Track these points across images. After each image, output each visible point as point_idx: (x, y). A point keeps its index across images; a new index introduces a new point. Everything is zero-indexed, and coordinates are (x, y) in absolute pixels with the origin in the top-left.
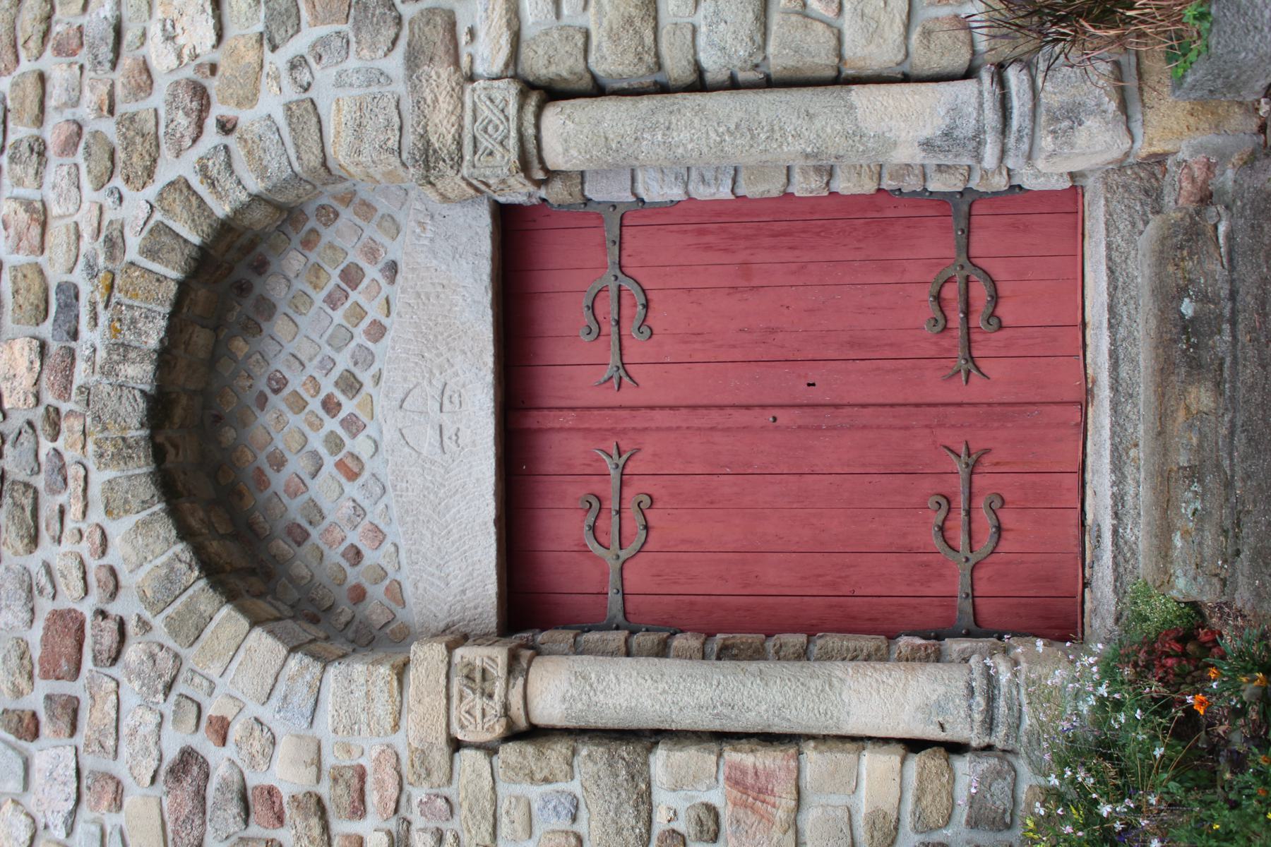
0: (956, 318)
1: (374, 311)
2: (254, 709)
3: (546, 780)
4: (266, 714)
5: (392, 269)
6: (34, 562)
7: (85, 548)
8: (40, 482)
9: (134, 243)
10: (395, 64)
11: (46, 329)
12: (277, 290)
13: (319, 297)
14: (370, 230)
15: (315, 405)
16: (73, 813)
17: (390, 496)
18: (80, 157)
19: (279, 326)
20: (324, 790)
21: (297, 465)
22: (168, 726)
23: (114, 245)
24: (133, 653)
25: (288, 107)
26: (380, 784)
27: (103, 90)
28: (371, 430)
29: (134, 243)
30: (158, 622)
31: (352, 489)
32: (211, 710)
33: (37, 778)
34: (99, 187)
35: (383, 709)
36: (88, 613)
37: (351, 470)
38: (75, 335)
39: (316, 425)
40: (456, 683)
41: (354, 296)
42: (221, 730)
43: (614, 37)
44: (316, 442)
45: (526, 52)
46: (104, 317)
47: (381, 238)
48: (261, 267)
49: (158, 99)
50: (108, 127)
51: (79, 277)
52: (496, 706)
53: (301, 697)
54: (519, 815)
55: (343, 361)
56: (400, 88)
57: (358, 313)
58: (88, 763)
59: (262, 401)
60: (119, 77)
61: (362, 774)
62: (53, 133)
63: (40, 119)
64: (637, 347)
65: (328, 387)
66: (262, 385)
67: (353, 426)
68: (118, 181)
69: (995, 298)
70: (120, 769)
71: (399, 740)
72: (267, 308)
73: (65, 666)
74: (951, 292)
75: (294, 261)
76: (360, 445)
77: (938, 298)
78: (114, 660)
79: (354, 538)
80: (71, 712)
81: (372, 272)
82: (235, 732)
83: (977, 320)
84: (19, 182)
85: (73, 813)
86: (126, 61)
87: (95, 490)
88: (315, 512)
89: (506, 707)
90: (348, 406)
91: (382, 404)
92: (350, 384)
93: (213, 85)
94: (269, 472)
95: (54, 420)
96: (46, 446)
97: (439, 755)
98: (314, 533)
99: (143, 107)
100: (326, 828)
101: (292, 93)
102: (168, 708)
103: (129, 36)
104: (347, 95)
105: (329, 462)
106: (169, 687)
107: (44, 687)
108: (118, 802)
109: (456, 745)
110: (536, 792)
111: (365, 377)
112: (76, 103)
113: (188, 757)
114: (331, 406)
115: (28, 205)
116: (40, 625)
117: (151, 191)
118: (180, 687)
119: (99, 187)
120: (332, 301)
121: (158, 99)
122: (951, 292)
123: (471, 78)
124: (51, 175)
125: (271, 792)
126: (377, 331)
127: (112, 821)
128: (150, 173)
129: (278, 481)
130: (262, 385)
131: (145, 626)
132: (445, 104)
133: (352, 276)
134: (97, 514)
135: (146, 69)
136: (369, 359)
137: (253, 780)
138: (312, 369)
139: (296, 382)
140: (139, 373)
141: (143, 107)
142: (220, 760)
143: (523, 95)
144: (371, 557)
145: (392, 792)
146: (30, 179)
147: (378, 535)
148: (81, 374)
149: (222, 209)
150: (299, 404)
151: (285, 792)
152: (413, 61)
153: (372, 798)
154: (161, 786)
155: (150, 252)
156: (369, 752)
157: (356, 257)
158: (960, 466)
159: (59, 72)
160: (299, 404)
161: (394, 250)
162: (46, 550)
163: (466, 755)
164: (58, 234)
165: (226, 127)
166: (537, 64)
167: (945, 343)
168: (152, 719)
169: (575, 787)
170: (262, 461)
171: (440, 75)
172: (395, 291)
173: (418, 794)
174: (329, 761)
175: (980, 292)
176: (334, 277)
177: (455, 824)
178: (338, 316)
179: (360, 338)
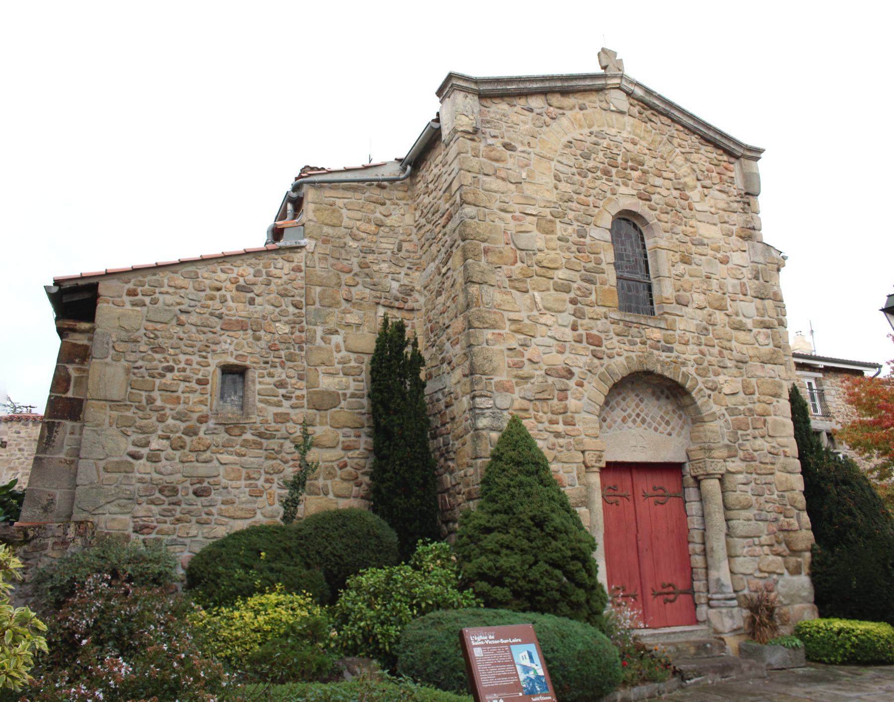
0: (666, 590)
1: (660, 429)
2: (586, 395)
3: (578, 478)
4: (585, 398)
5: (670, 434)
6: (612, 334)
7: (617, 349)
8: (630, 338)
9: (684, 369)
10: (726, 442)
11: (663, 343)
12: (663, 401)
13: (662, 413)
14: (677, 429)
15: (637, 411)
16: (555, 338)
17: (619, 431)
18: (699, 355)
19: (656, 402)
20: (569, 414)
21: (623, 404)
22: (580, 370)
23: (684, 364)
24: (596, 361)
25: (714, 413)
26: (574, 430)
27: (714, 363)
28: (634, 427)
29: (684, 369)
30: (603, 369)
31: (619, 420)
32: (585, 382)
33: (563, 329)
34: (695, 360)
35: (590, 432)
36: (603, 348)
37: (624, 420)
38: (663, 351)
39: (633, 410)
40: (598, 453)
41: (663, 423)
42: (580, 385)
43: (737, 498)
44: (629, 411)
45: (731, 475)
46: (668, 360)
47: (676, 431)
48: (667, 398)
49: (713, 378)
50: (706, 364)
51: (674, 354)
52: (594, 464)
53: (591, 409)
54: (570, 469)
55: (648, 419)
56: (722, 443)
57: (660, 425)
58: (568, 344)
59: (637, 396)
60: (716, 367)
61: (574, 425)
62: (703, 347)
63: (706, 345)
64: (652, 499)
65: (642, 415)
66: (641, 396)
67: (634, 421)
68: (696, 366)
69: (671, 601)
70: (567, 354)
71: (583, 436)
72: (658, 399)
73: (591, 341)
74: (671, 589)
75: (670, 408)
76: (630, 423)
77: (670, 585)
78: (594, 356)
79: (608, 420)
80: (580, 342)
81: (669, 429)
82: (580, 389)
83: (666, 596)
84: (693, 338)
85: (555, 338)
86: (720, 370)
87: (631, 354)
88: (613, 409)
89: (593, 467)
90: (639, 420)
91: (640, 430)
92: (643, 421)
93: (716, 392)
94: (621, 396)
95: (644, 343)
96: (638, 340)
97: (581, 448)
98: (608, 409)
99: (711, 374)
100: (560, 413)
101: (718, 413)
102: (583, 370)
103: (725, 370)
104: (718, 429)
105: (625, 414)
106: (590, 371)
107: (584, 333)
108: (559, 352)
109: (583, 452)
110: (575, 474)
111: (645, 426)
112: (710, 355)
113: (571, 374)
114: (638, 415)
115: (688, 341)
116: (597, 333)
117: (695, 375)
118: (589, 374)
119: (695, 360)
120: (662, 417)
121: (713, 378)
122: (671, 589)
123: (725, 461)
124: (695, 347)
125: (567, 398)
126: (656, 429)
127: (554, 349)
128: (699, 375)
129: (619, 399)
130: (641, 396)
131: (602, 365)
132: (720, 454)
133: (668, 423)
134: (625, 354)
135: (719, 374)
136: (650, 427)
137: (569, 393)
138: (646, 410)
139: (642, 405)
140: (658, 369)
141: (711, 374)
142: (572, 383)
143: (722, 475)
144: (605, 424)
145: (572, 433)
146: (694, 341)
147: (610, 427)
148: (656, 352)
149: (693, 394)
150: (637, 406)
151: (567, 402)
152: (728, 446)
153: (569, 428)
154: (565, 366)
155: (683, 374)
156: (580, 427)
157: (672, 424)
158: (633, 593)
159: (716, 350)
160: (637, 406)
161: (674, 435)
162: (616, 338)
163: (581, 455)
164: (683, 348)
165: (709, 396)
166: (729, 479)
167: (660, 588)
168: (581, 365)
169: (577, 486)
170: (624, 395)
171: (725, 453)
172: (664, 435)
173: (572, 440)
174: (576, 415)
175: (672, 597)
176: (667, 418)
177: (565, 451)
178: (658, 419)
179: (654, 425)
